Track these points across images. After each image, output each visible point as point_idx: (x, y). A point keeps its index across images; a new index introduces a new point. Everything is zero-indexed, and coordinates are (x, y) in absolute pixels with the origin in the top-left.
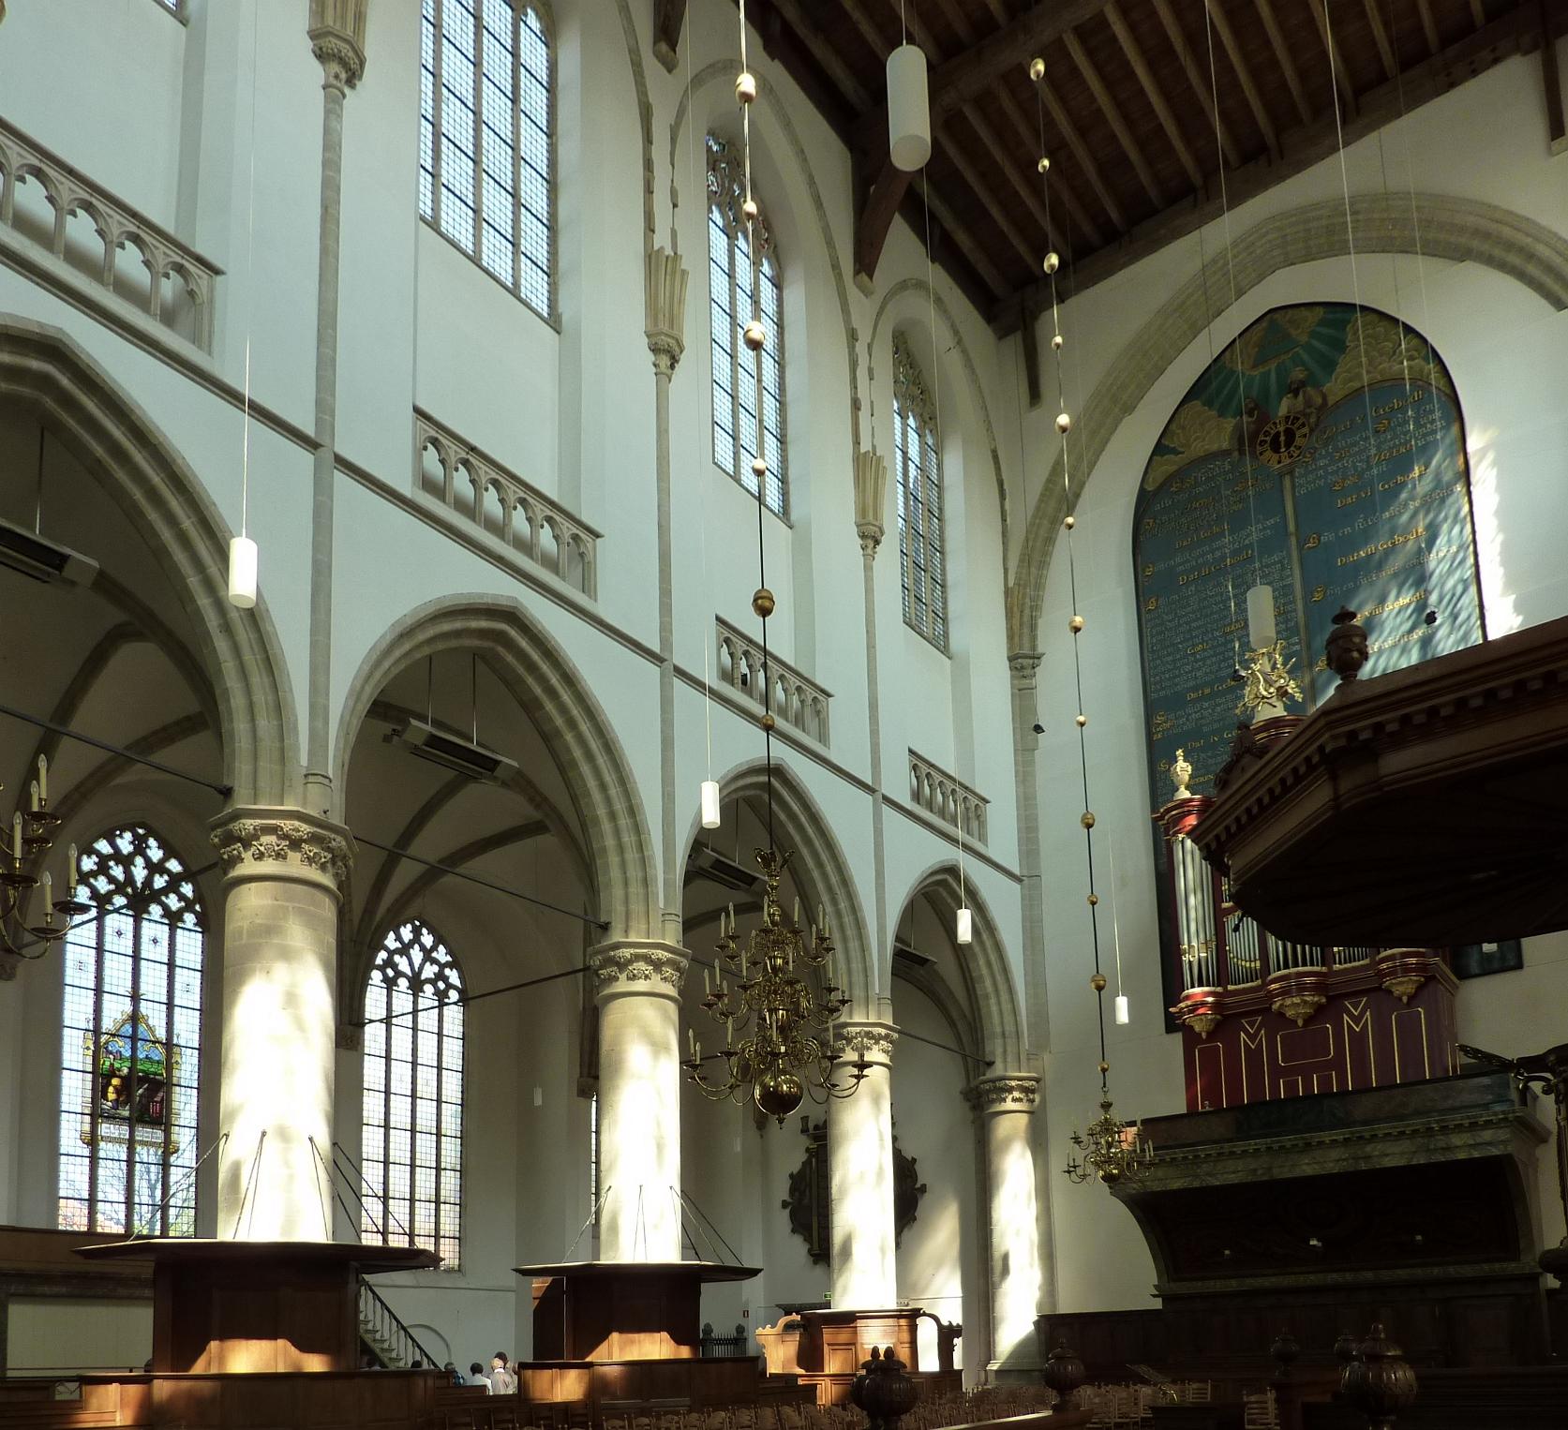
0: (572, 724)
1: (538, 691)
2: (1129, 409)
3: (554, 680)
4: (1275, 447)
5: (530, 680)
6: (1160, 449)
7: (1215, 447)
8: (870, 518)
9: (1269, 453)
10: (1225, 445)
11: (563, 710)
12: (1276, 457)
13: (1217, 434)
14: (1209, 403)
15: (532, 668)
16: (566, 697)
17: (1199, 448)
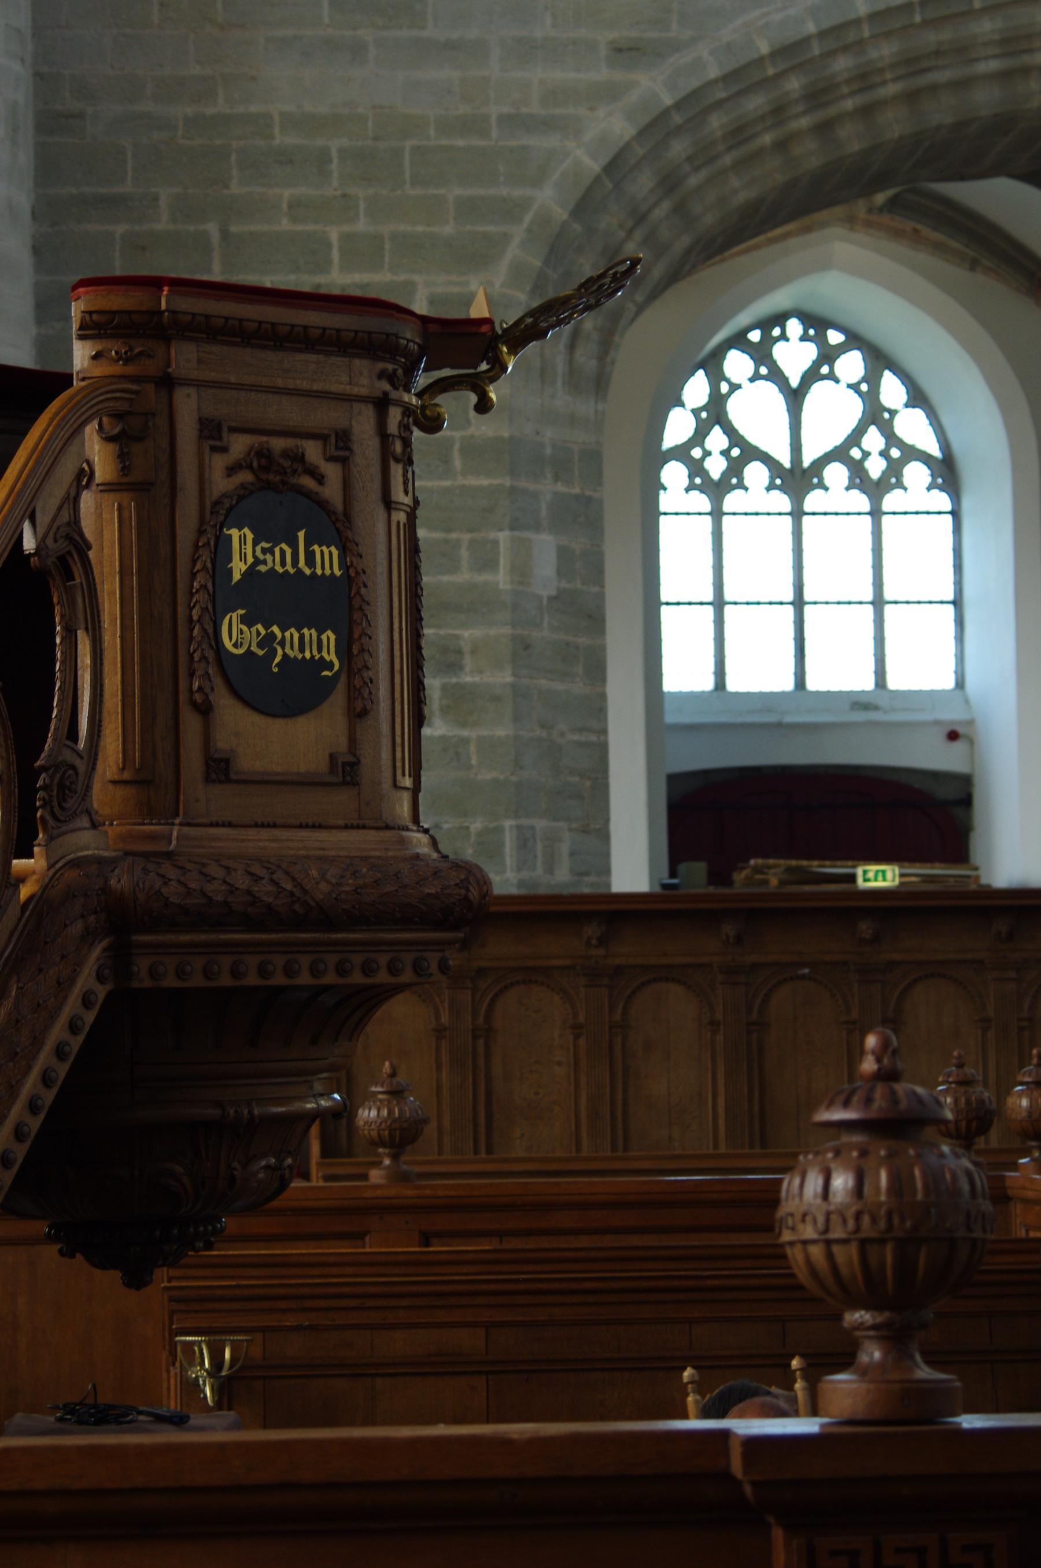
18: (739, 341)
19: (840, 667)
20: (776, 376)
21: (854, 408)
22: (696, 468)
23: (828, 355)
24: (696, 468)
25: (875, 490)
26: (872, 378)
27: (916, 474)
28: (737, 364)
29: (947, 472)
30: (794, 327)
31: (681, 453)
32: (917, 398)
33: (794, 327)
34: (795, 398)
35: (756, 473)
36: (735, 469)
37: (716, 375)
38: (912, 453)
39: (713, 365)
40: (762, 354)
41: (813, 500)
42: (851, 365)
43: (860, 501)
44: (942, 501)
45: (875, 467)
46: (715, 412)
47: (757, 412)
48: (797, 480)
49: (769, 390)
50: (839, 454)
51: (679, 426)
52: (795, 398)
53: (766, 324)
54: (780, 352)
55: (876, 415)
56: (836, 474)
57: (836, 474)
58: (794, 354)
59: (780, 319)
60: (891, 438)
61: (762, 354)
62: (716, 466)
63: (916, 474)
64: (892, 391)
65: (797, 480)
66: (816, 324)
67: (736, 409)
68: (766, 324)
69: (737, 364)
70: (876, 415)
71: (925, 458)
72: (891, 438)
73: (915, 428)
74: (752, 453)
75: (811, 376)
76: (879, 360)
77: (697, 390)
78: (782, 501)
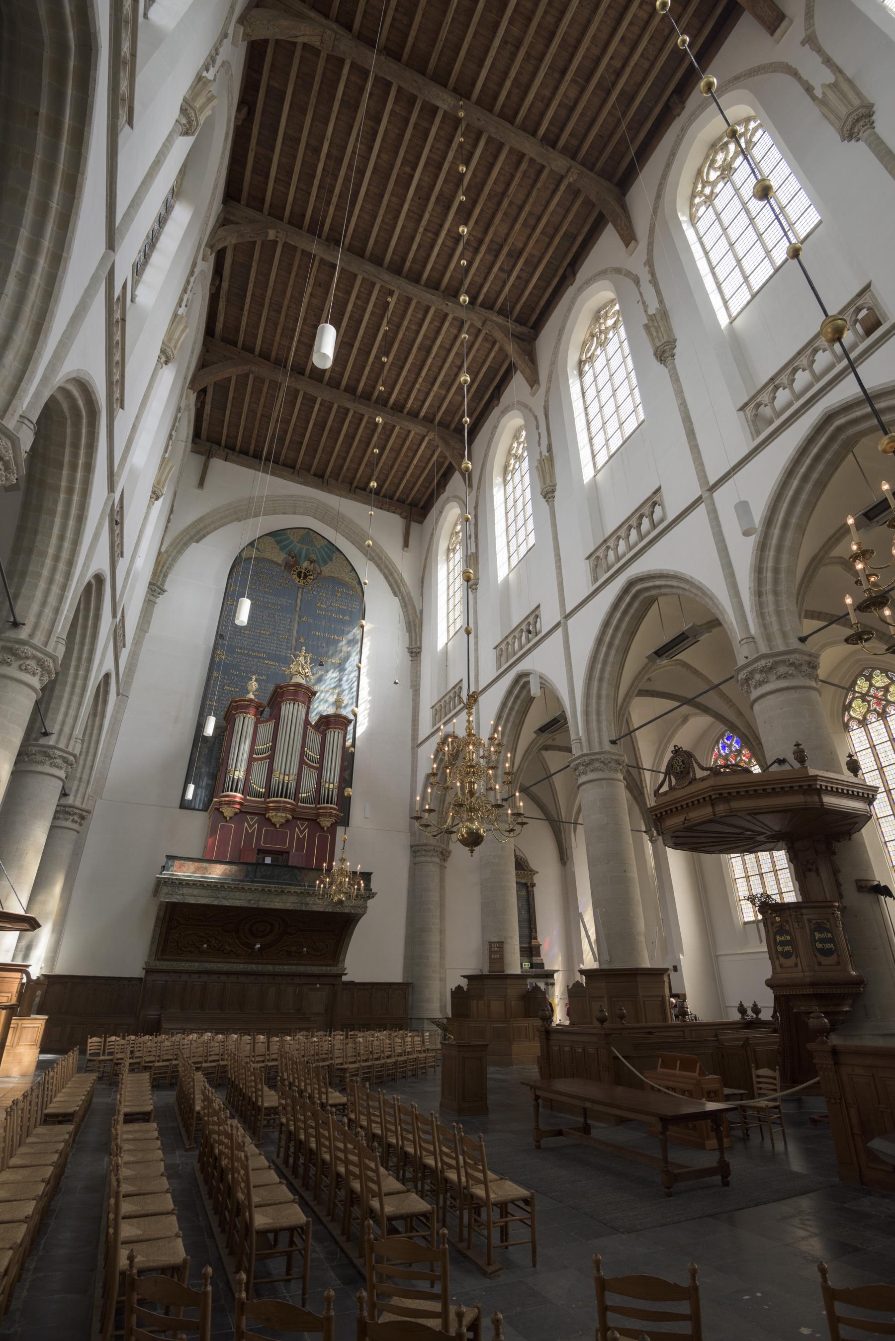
0: (70, 491)
1: (67, 459)
2: (239, 520)
3: (81, 461)
4: (299, 577)
5: (68, 450)
6: (251, 544)
7: (275, 560)
8: (160, 487)
9: (295, 576)
10: (280, 562)
11: (72, 480)
12: (298, 579)
13: (280, 557)
14: (278, 543)
15: (76, 446)
16: (79, 475)
17: (267, 555)
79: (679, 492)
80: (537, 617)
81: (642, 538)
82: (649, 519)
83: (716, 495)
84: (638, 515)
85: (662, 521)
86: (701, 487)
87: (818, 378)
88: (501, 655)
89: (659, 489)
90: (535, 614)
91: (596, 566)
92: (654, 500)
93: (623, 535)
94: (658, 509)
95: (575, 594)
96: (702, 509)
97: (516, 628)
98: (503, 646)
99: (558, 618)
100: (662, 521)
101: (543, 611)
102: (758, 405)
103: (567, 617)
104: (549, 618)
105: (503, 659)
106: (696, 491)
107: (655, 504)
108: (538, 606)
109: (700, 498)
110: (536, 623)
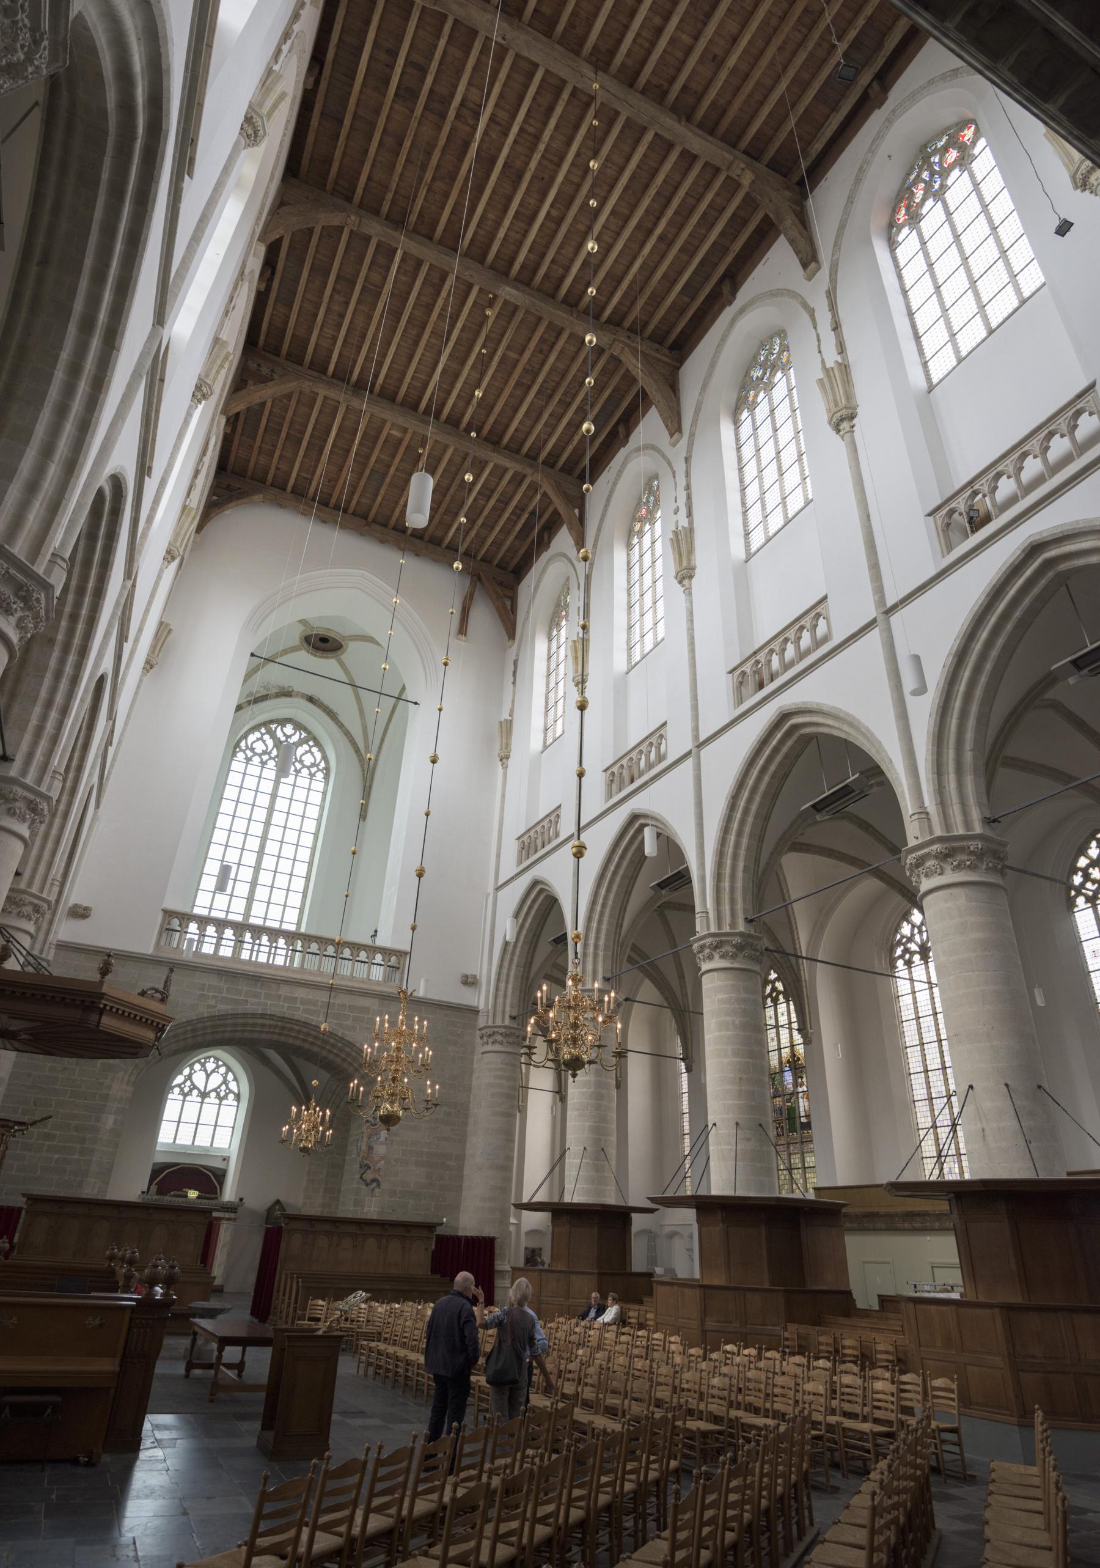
18: (198, 1061)
19: (203, 1140)
20: (205, 1070)
21: (221, 1079)
22: (182, 1090)
23: (218, 1067)
24: (182, 1090)
25: (221, 1099)
26: (226, 1073)
27: (231, 1096)
28: (197, 1067)
29: (238, 1097)
30: (212, 1060)
31: (179, 1086)
32: (235, 1079)
33: (212, 1060)
34: (208, 1076)
35: (195, 1092)
36: (191, 1091)
37: (192, 1069)
38: (231, 1091)
39: (192, 1067)
40: (203, 1065)
41: (207, 1100)
42: (223, 1070)
43: (217, 1101)
44: (235, 1103)
45: (222, 1094)
46: (189, 1077)
47: (199, 1078)
48: (204, 1095)
49: (203, 1073)
50: (215, 1090)
51: (179, 1079)
52: (208, 1076)
53: (205, 1058)
54: (207, 1065)
55: (225, 1082)
56: (213, 1094)
57: (213, 1094)
58: (210, 1066)
59: (209, 1057)
60: (227, 1088)
61: (203, 1065)
62: (186, 1090)
63: (231, 1096)
64: (230, 1077)
65: (204, 1095)
66: (217, 1059)
67: (194, 1077)
68: (205, 1058)
69: (197, 1067)
70: (225, 1082)
71: (234, 1093)
72: (227, 1088)
73: (233, 1086)
74: (195, 1087)
75: (213, 1071)
76: (229, 1069)
77: (186, 1071)
78: (199, 1099)
79: (850, 610)
80: (661, 736)
81: (802, 656)
82: (808, 636)
83: (895, 619)
84: (797, 624)
85: (826, 639)
86: (876, 609)
87: (1054, 469)
88: (612, 781)
89: (825, 598)
90: (659, 733)
91: (741, 683)
92: (817, 610)
93: (777, 649)
94: (822, 622)
95: (713, 717)
96: (875, 634)
97: (634, 748)
98: (615, 769)
99: (688, 745)
100: (826, 639)
101: (669, 731)
102: (975, 493)
103: (701, 745)
104: (677, 743)
105: (614, 787)
106: (871, 612)
107: (818, 615)
108: (665, 724)
109: (874, 621)
110: (660, 744)
